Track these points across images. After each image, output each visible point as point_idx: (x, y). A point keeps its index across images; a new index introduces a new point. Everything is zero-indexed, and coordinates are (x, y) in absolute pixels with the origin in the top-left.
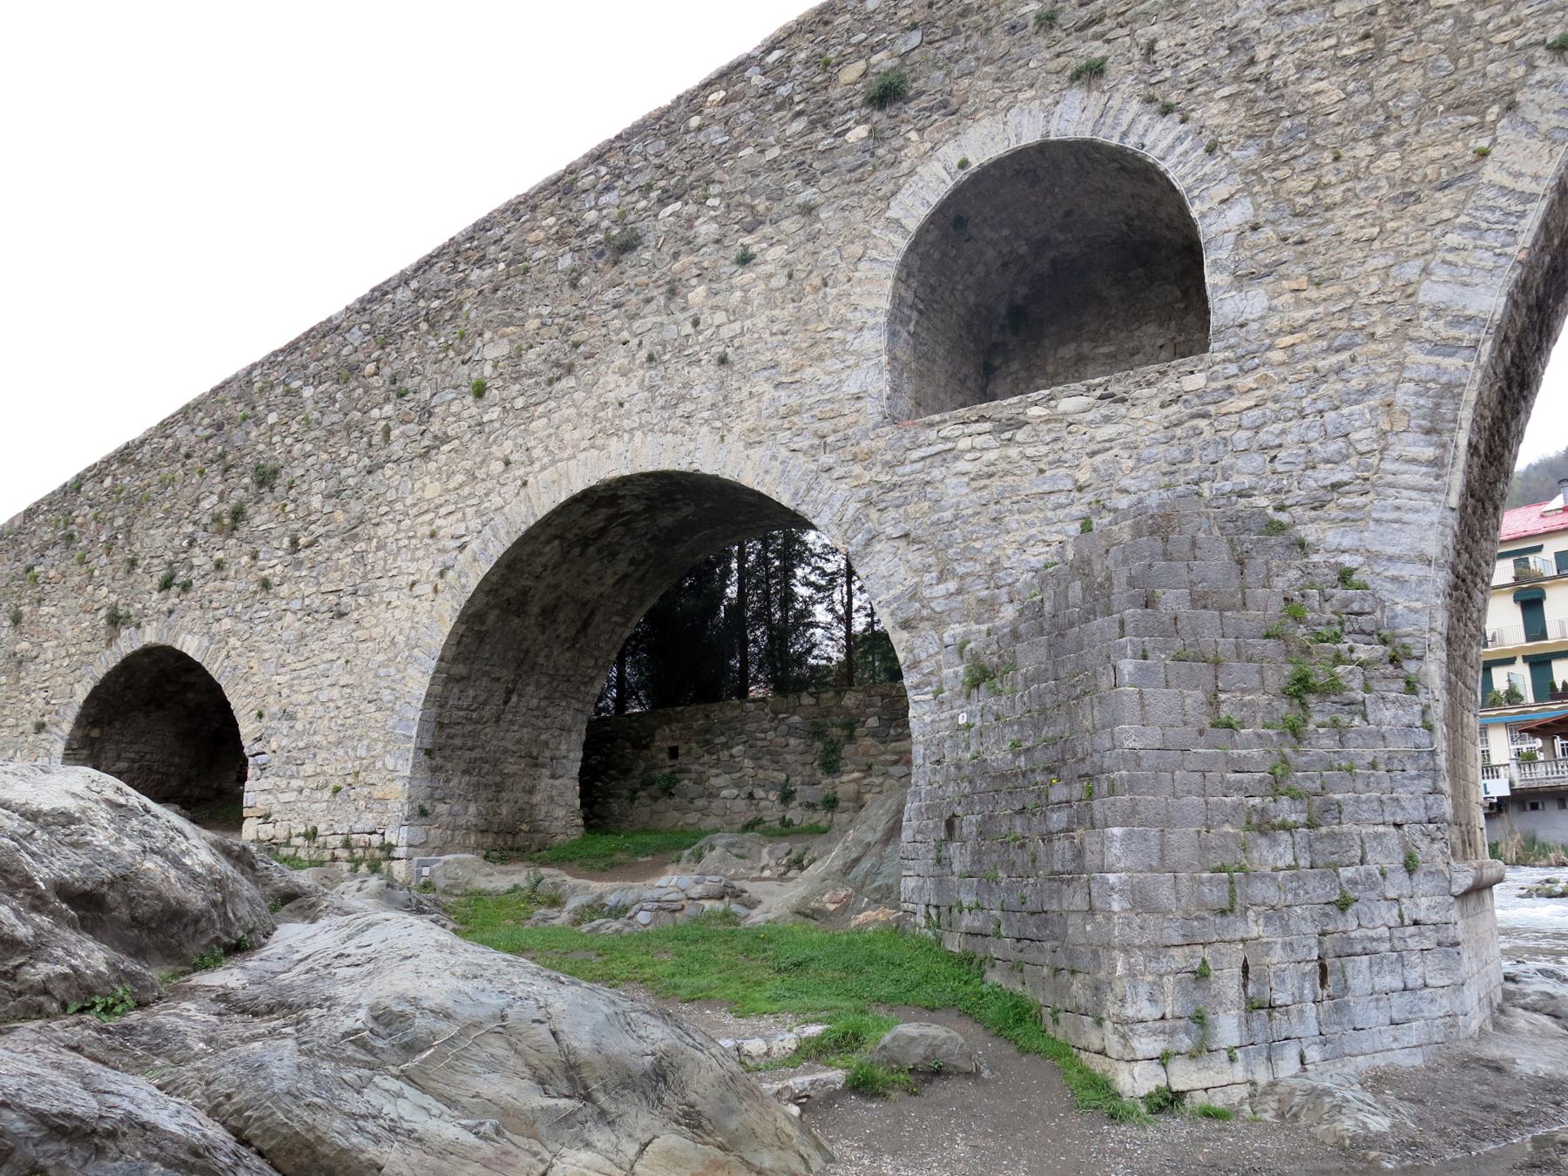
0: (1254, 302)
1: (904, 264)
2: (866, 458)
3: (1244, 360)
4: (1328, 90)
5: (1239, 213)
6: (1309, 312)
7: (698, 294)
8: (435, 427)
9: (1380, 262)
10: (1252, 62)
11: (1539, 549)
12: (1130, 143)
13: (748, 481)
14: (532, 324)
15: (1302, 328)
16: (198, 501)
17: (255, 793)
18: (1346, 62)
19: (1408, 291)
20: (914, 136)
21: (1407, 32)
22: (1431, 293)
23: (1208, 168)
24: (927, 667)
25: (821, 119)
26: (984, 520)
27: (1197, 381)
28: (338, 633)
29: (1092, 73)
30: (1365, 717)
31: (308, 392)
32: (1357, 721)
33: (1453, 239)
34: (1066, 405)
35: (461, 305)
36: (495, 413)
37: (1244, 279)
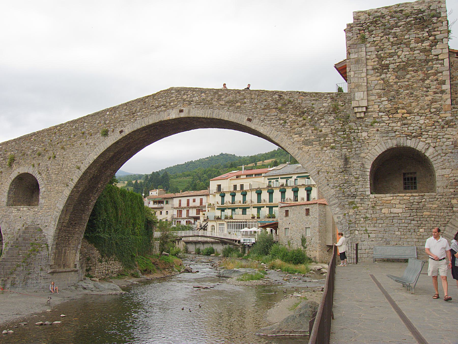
1: (11, 184)
4: (54, 176)
5: (44, 189)
6: (47, 204)
9: (54, 200)
10: (48, 170)
11: (291, 177)
12: (35, 176)
15: (46, 206)
18: (56, 174)
20: (14, 166)
21: (61, 172)
22: (58, 205)
23: (42, 183)
24: (6, 240)
26: (14, 222)
27: (36, 210)
30: (40, 254)
32: (39, 254)
33: (60, 199)
34: (25, 209)
37: (43, 198)
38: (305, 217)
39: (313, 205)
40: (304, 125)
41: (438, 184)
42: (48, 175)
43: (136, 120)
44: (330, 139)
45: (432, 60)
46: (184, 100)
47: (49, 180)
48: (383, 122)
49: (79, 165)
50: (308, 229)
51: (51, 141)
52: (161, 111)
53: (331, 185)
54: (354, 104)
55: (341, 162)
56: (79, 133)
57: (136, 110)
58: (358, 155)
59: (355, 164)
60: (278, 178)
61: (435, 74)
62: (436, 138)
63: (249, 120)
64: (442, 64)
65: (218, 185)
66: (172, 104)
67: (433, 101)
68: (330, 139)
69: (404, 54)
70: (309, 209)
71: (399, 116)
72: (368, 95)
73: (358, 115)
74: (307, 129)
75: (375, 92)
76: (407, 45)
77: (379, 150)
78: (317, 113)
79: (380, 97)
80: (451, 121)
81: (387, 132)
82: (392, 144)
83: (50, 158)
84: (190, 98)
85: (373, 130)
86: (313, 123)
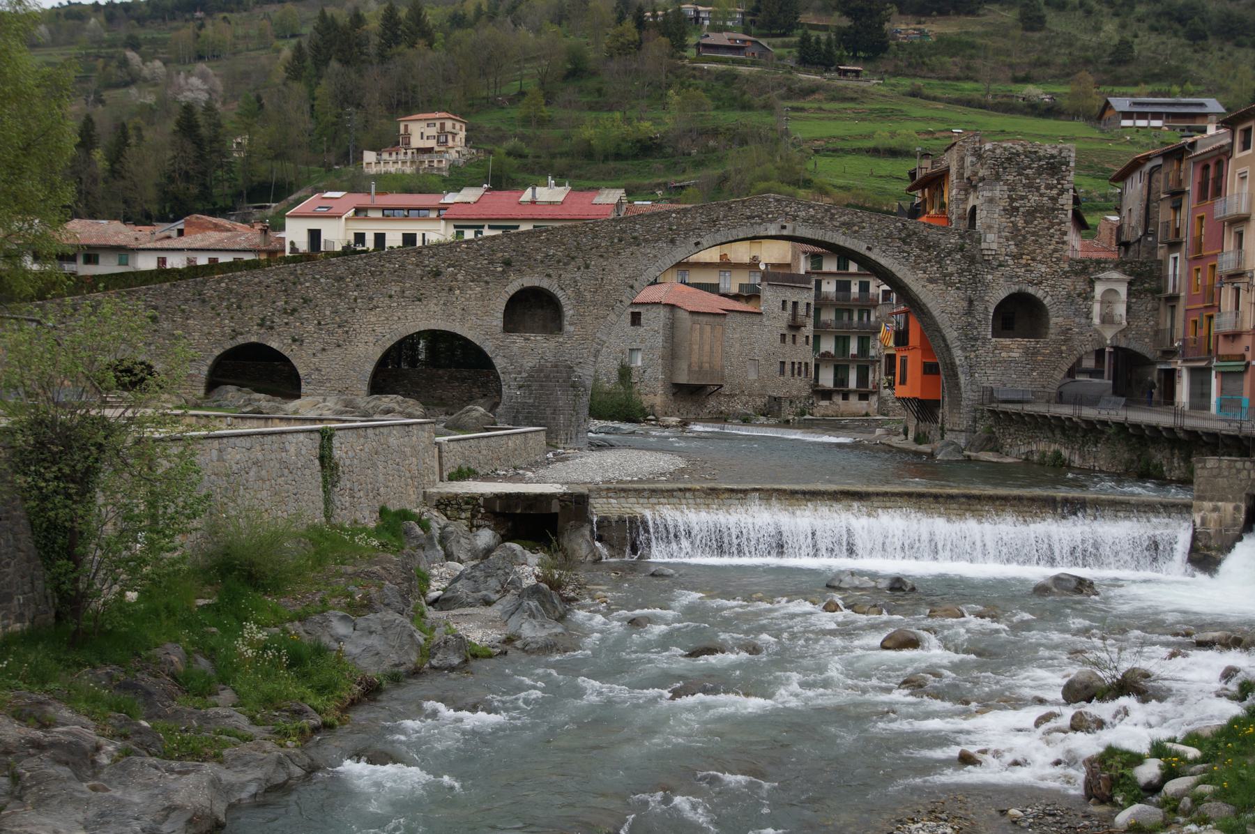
0: (572, 329)
2: (497, 339)
3: (570, 338)
4: (588, 295)
5: (571, 312)
7: (457, 292)
8: (375, 302)
13: (469, 337)
14: (408, 285)
16: (274, 302)
17: (304, 388)
19: (595, 333)
22: (598, 335)
25: (491, 262)
27: (561, 340)
28: (338, 351)
29: (549, 276)
31: (322, 280)
35: (382, 272)
36: (395, 304)
38: (629, 329)
39: (649, 307)
40: (929, 261)
41: (1052, 331)
42: (578, 293)
43: (719, 230)
44: (955, 278)
45: (1058, 209)
46: (787, 214)
47: (579, 299)
48: (1008, 266)
49: (631, 282)
50: (634, 354)
51: (578, 244)
52: (756, 223)
53: (955, 327)
54: (984, 245)
55: (965, 304)
56: (627, 236)
57: (718, 218)
58: (982, 299)
59: (979, 307)
60: (483, 227)
61: (1059, 224)
62: (1053, 286)
63: (869, 249)
64: (1066, 215)
65: (309, 230)
66: (770, 216)
67: (1055, 251)
68: (955, 278)
69: (1034, 198)
70: (639, 314)
71: (1024, 262)
72: (999, 237)
73: (986, 258)
74: (932, 266)
75: (1003, 234)
76: (1038, 189)
77: (1003, 294)
78: (944, 250)
79: (1008, 240)
80: (1068, 272)
81: (1012, 277)
82: (1015, 289)
83: (579, 268)
84: (795, 211)
85: (998, 274)
86: (940, 261)
